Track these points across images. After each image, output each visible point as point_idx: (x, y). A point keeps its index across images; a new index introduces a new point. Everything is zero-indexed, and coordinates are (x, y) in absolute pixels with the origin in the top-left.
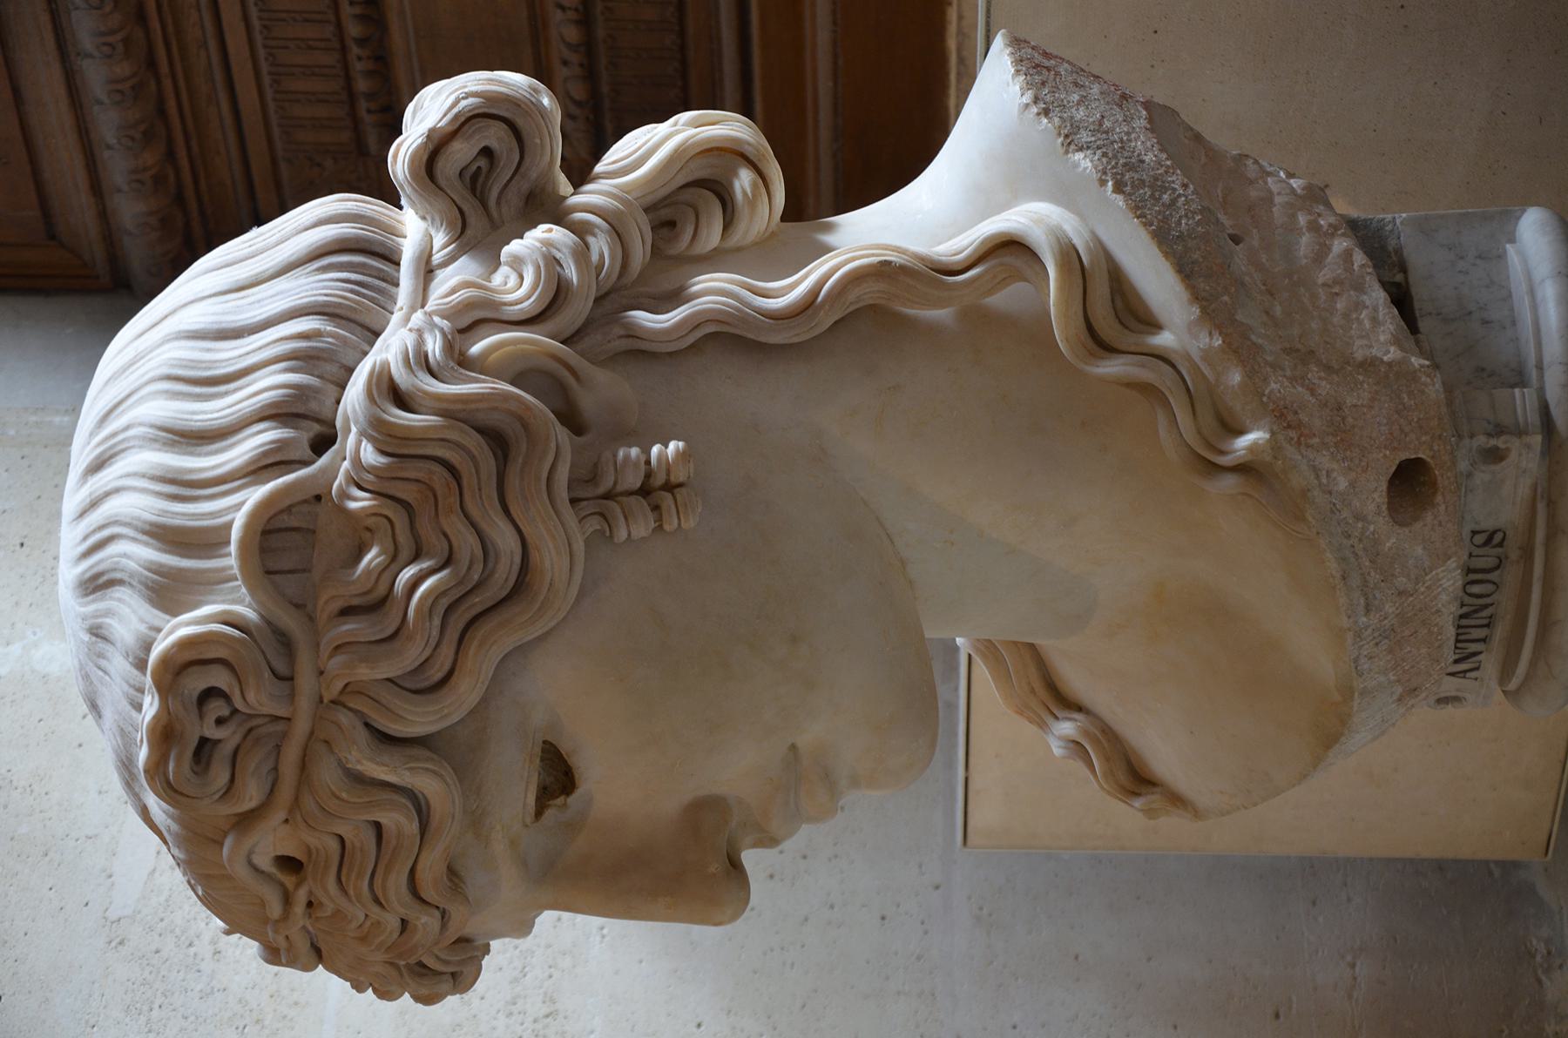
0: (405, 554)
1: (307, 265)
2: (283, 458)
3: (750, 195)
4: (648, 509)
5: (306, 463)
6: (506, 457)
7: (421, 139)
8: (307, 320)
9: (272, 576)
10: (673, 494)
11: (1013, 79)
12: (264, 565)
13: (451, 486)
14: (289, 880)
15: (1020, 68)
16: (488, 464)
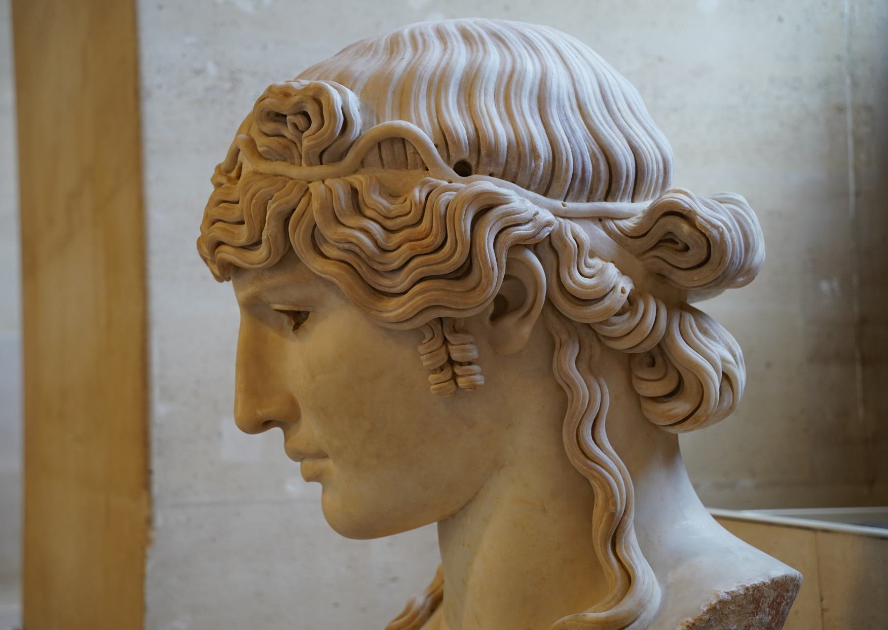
0: (389, 224)
1: (597, 146)
2: (449, 146)
3: (669, 413)
4: (440, 364)
5: (448, 159)
6: (458, 279)
7: (688, 207)
8: (548, 151)
9: (377, 146)
10: (450, 380)
11: (741, 586)
12: (383, 141)
13: (428, 248)
14: (233, 174)
15: (751, 590)
16: (444, 268)
